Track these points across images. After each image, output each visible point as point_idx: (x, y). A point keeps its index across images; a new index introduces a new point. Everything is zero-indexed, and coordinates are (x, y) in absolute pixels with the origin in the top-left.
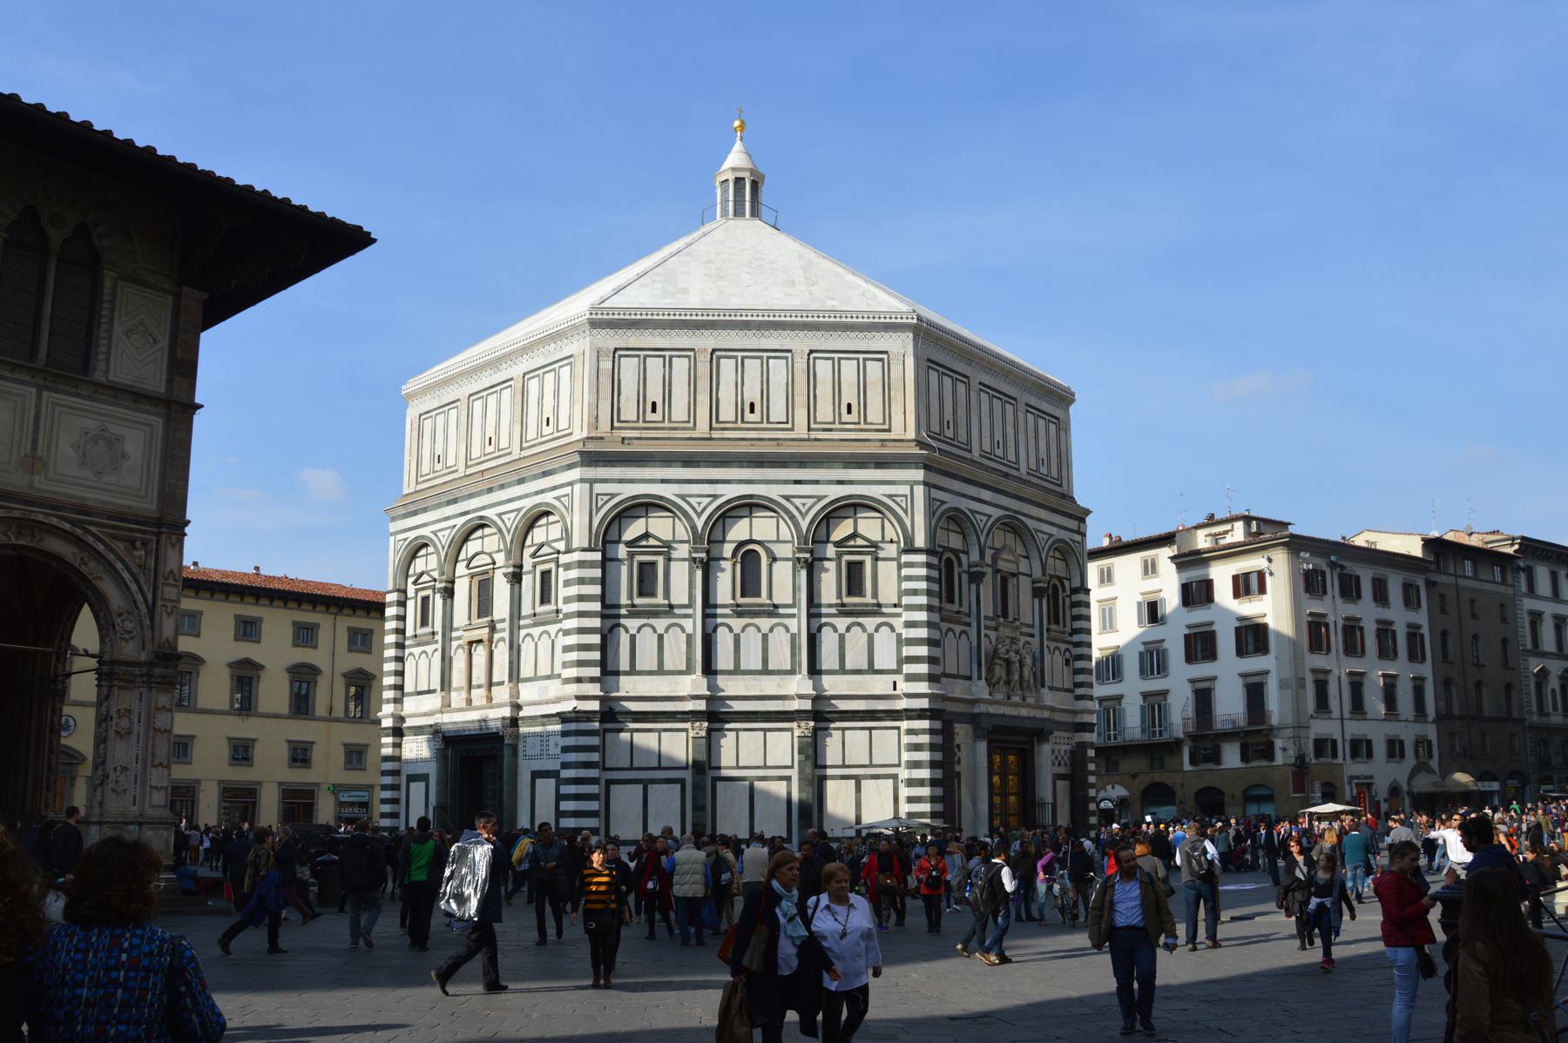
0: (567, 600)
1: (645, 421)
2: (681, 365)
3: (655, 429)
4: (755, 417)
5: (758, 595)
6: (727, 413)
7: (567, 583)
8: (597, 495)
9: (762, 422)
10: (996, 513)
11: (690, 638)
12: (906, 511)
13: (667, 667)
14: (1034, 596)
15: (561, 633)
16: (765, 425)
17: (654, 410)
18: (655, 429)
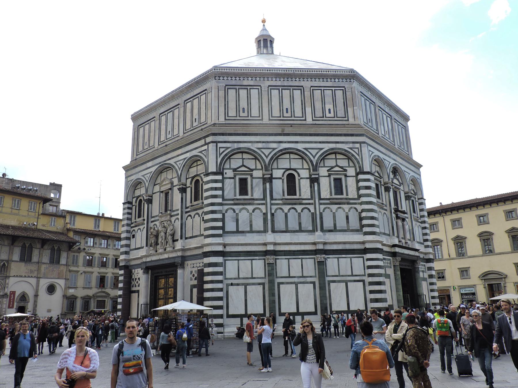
0: (207, 198)
1: (239, 116)
2: (254, 93)
3: (244, 120)
7: (207, 190)
8: (220, 148)
9: (291, 117)
10: (393, 162)
11: (265, 214)
12: (359, 156)
13: (254, 230)
14: (406, 200)
15: (203, 214)
16: (293, 118)
17: (244, 112)
18: (244, 120)
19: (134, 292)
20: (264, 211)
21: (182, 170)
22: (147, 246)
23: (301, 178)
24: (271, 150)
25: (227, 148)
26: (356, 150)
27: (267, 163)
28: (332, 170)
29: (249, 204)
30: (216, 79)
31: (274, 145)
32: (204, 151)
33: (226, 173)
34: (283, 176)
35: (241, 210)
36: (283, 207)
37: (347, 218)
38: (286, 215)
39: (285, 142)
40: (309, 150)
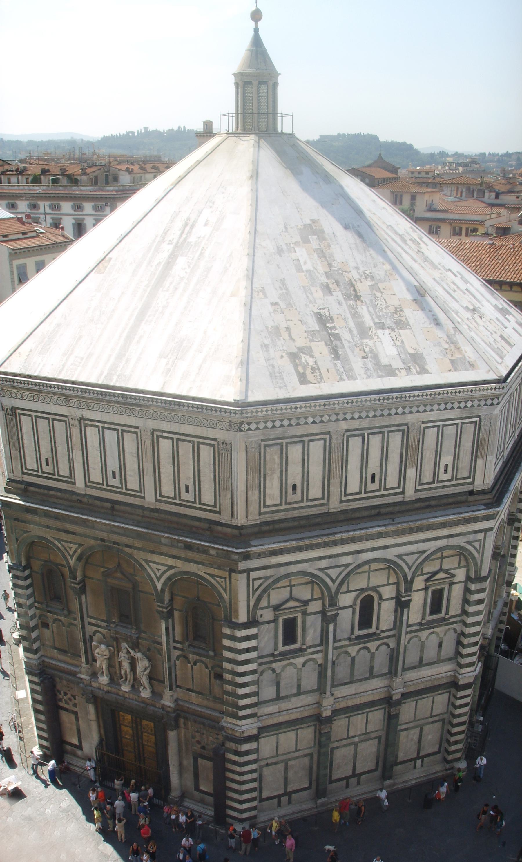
1: (287, 504)
4: (375, 486)
5: (371, 627)
6: (353, 486)
8: (254, 580)
19: (66, 710)
20: (320, 662)
21: (165, 584)
22: (87, 663)
23: (385, 600)
24: (342, 568)
25: (267, 578)
26: (477, 545)
27: (333, 591)
28: (433, 579)
29: (298, 657)
30: (242, 431)
31: (348, 559)
32: (222, 580)
33: (261, 616)
34: (355, 604)
35: (284, 668)
36: (349, 649)
37: (440, 644)
38: (353, 659)
39: (367, 551)
40: (404, 557)
